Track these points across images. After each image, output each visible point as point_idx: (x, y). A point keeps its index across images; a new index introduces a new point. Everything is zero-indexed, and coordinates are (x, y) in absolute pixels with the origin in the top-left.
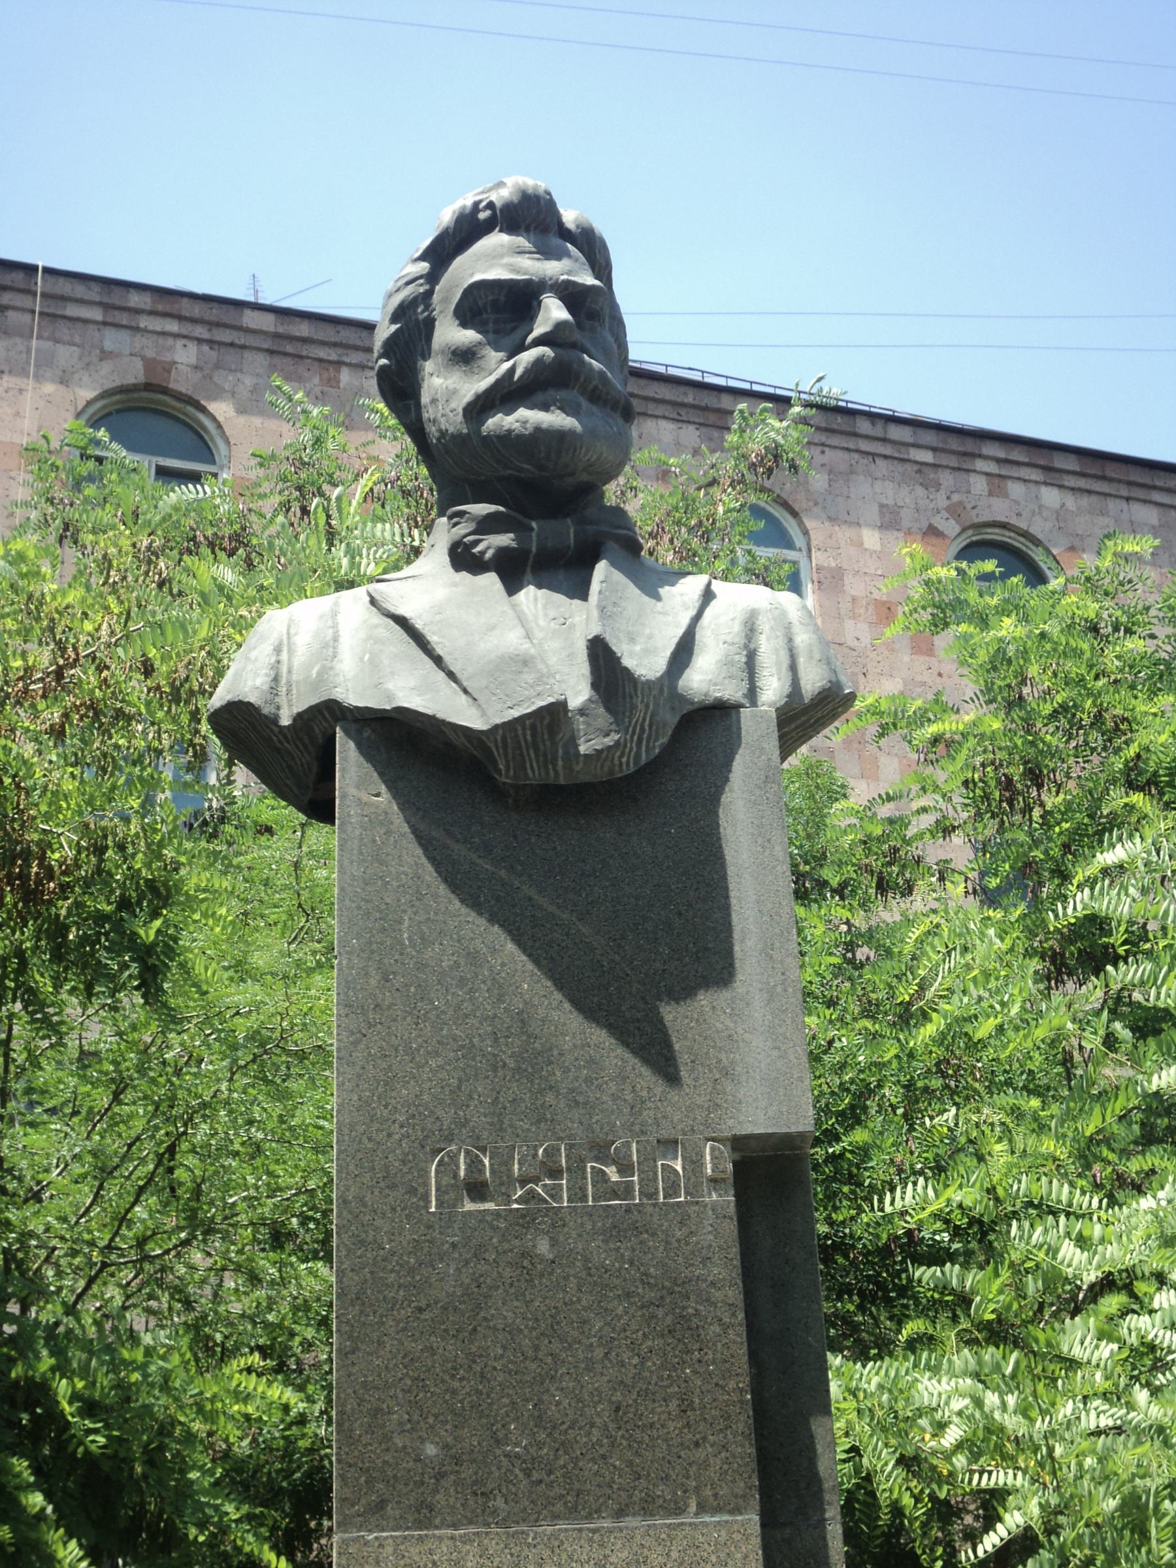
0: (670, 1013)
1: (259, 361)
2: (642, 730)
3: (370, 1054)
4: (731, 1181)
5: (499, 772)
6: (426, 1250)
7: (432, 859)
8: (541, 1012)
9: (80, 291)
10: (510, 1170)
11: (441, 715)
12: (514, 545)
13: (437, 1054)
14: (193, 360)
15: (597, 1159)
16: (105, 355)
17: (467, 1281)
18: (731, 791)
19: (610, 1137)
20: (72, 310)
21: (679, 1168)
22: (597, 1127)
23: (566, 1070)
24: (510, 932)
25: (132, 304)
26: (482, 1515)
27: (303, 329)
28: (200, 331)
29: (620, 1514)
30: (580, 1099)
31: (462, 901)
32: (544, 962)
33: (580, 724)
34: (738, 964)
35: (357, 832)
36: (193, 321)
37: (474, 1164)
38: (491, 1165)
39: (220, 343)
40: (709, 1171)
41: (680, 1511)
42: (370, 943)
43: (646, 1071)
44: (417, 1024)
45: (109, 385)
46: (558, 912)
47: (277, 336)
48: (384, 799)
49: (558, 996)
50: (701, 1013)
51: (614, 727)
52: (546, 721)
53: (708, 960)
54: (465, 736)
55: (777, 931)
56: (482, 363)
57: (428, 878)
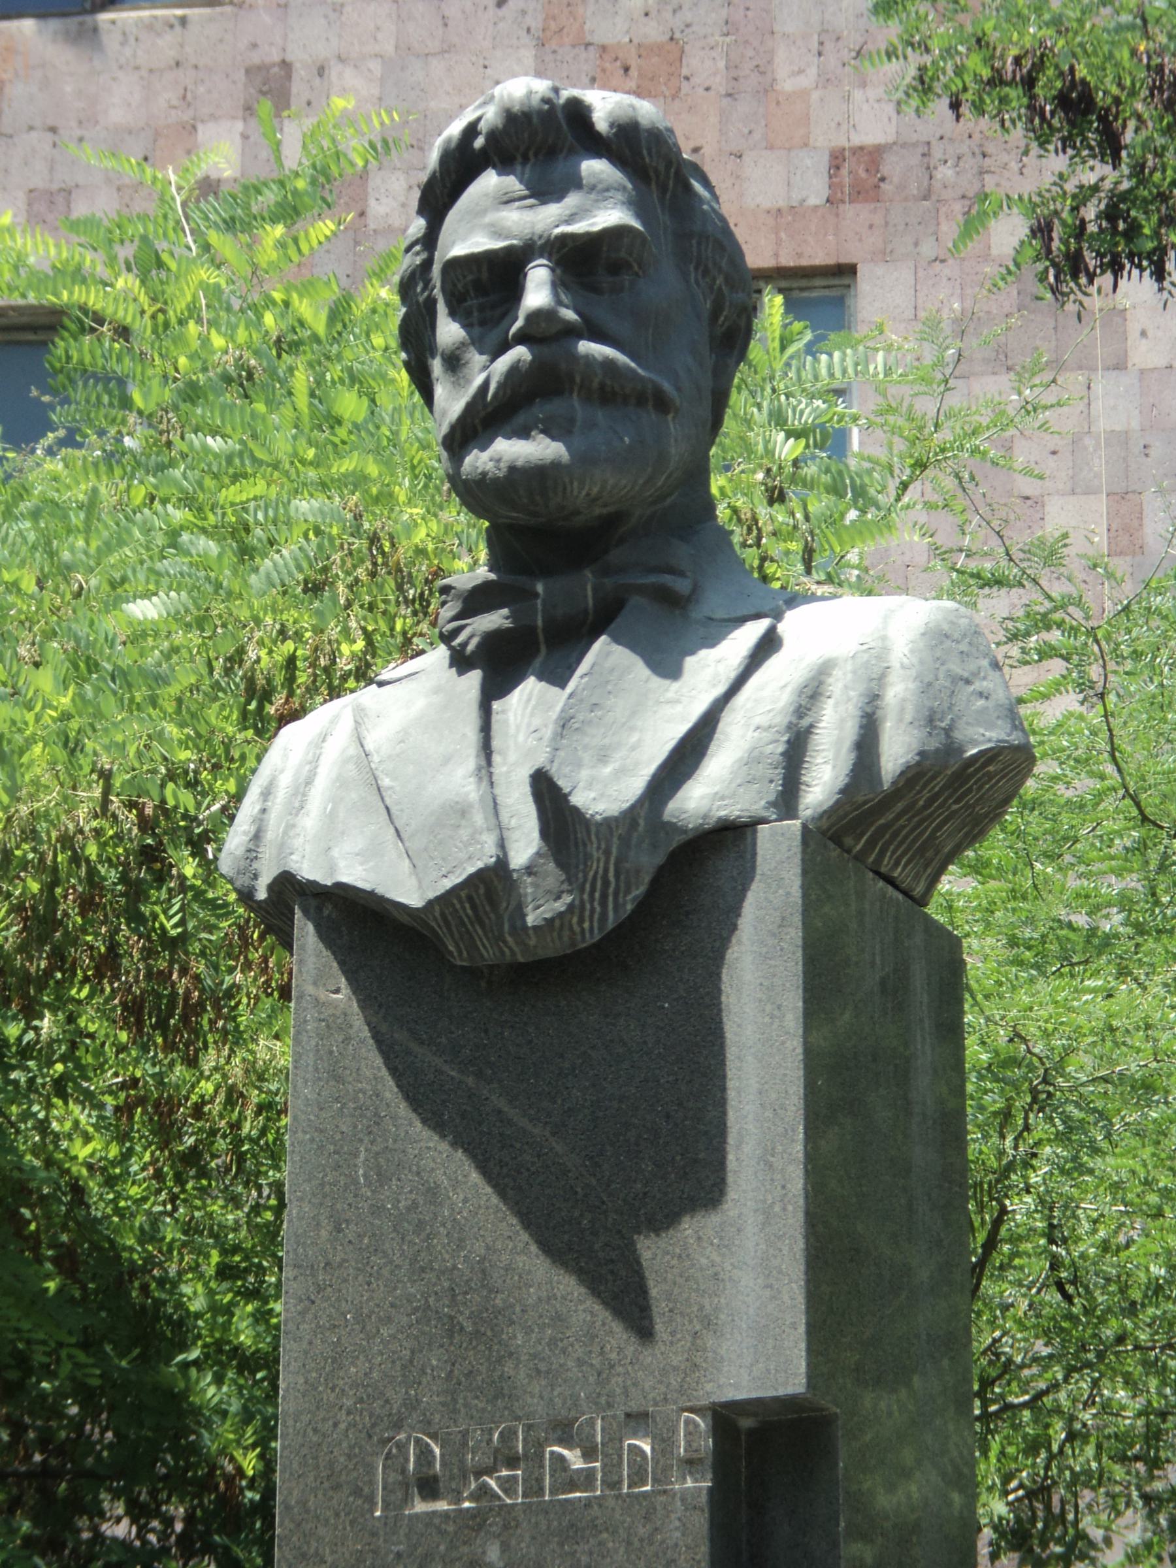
2: (606, 883)
4: (709, 1461)
5: (451, 953)
7: (393, 1071)
11: (380, 890)
12: (507, 624)
13: (389, 1319)
18: (739, 943)
19: (573, 1414)
23: (528, 1331)
30: (543, 1367)
31: (424, 1121)
32: (511, 1193)
33: (528, 887)
34: (730, 1179)
35: (313, 1043)
37: (425, 1454)
38: (442, 1455)
42: (322, 1185)
43: (617, 1327)
46: (529, 1127)
48: (343, 996)
49: (525, 1236)
50: (685, 1247)
51: (565, 886)
52: (482, 891)
53: (697, 1179)
54: (409, 915)
55: (780, 1130)
56: (466, 370)
57: (388, 1095)
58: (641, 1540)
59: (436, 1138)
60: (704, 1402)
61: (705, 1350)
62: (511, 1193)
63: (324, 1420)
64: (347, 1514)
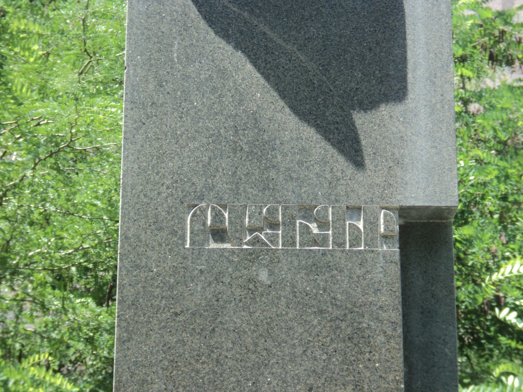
0: (361, 119)
3: (147, 137)
4: (397, 238)
6: (182, 273)
8: (269, 114)
10: (243, 222)
15: (304, 218)
17: (209, 297)
19: (314, 203)
21: (361, 225)
22: (305, 196)
23: (285, 155)
24: (249, 57)
30: (294, 175)
31: (216, 33)
32: (272, 79)
34: (409, 87)
38: (230, 218)
40: (382, 230)
42: (150, 59)
43: (341, 159)
44: (181, 118)
46: (284, 44)
49: (281, 103)
50: (382, 120)
53: (389, 84)
55: (439, 65)
57: (192, 15)
58: (358, 277)
59: (224, 42)
60: (396, 205)
61: (396, 177)
62: (272, 79)
63: (151, 190)
64: (168, 245)
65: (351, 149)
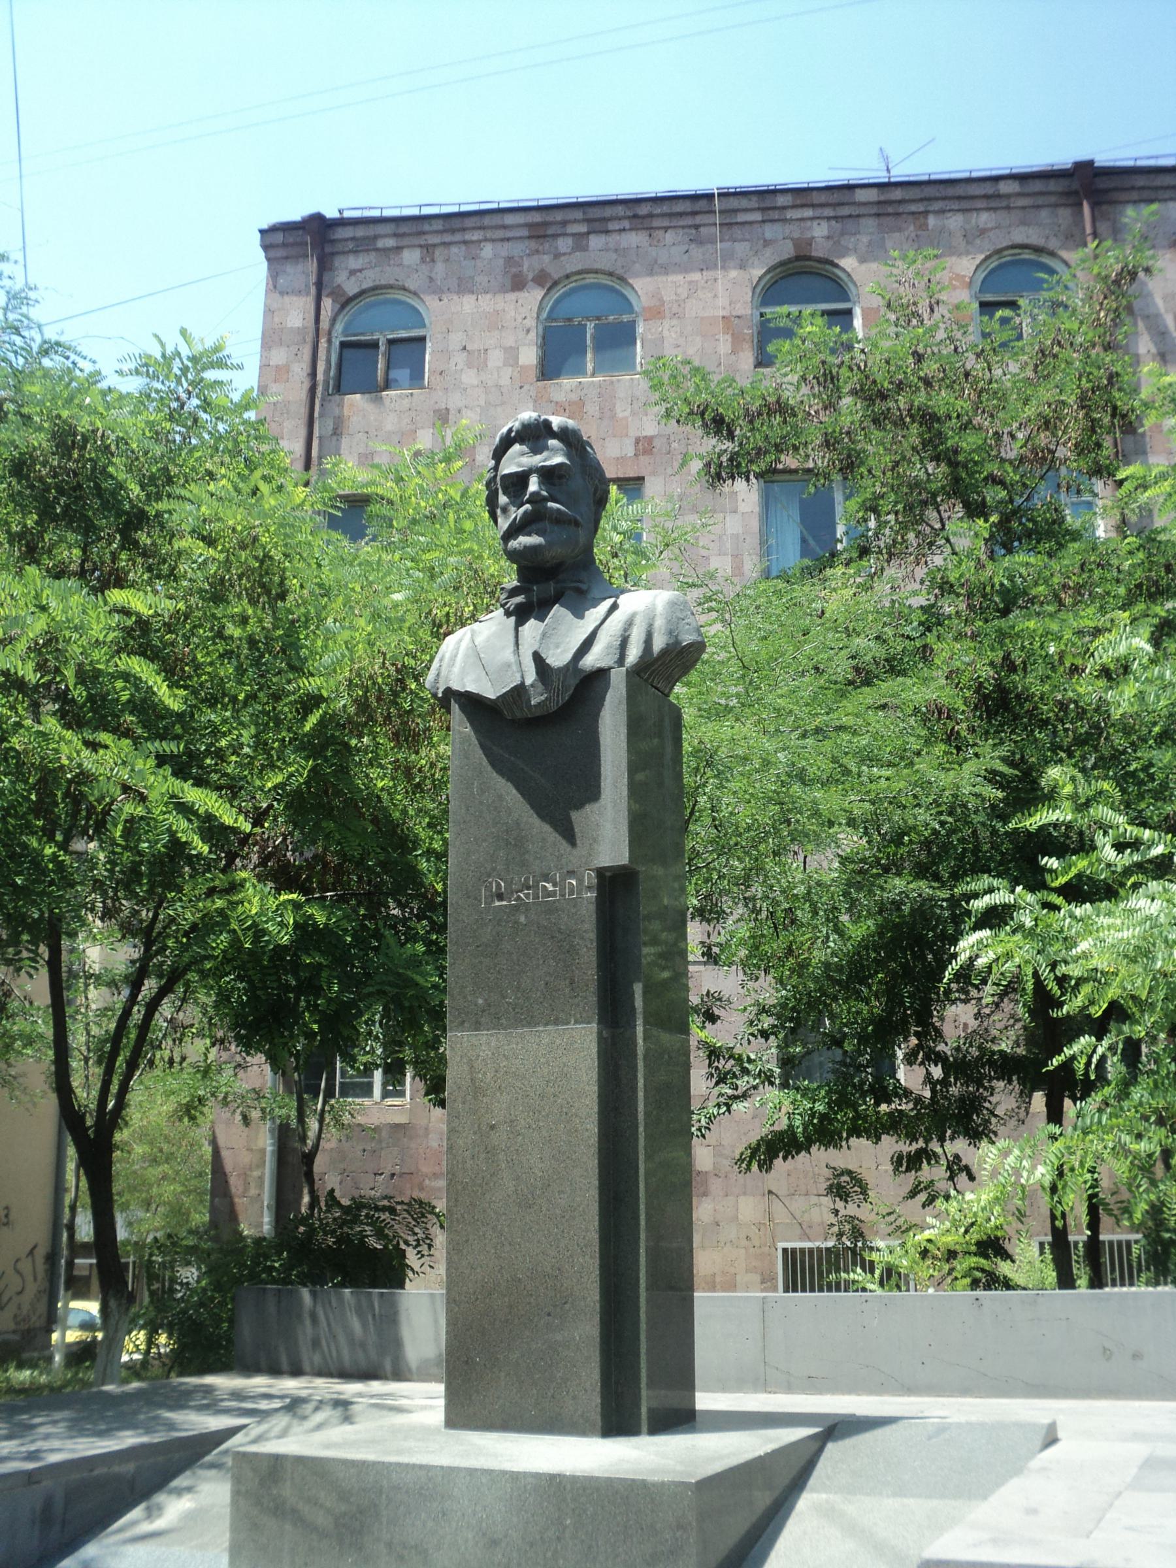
0: (575, 816)
1: (869, 224)
9: (744, 203)
14: (825, 233)
16: (767, 243)
20: (741, 218)
25: (779, 204)
26: (498, 1026)
27: (898, 194)
28: (828, 212)
29: (546, 1025)
36: (822, 205)
37: (498, 885)
39: (842, 217)
41: (568, 1023)
45: (772, 263)
47: (879, 203)
48: (468, 730)
53: (590, 791)
65: (569, 835)
